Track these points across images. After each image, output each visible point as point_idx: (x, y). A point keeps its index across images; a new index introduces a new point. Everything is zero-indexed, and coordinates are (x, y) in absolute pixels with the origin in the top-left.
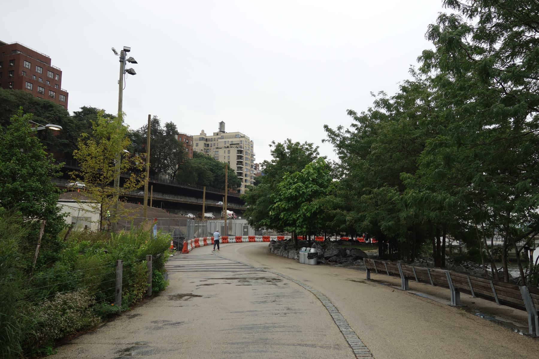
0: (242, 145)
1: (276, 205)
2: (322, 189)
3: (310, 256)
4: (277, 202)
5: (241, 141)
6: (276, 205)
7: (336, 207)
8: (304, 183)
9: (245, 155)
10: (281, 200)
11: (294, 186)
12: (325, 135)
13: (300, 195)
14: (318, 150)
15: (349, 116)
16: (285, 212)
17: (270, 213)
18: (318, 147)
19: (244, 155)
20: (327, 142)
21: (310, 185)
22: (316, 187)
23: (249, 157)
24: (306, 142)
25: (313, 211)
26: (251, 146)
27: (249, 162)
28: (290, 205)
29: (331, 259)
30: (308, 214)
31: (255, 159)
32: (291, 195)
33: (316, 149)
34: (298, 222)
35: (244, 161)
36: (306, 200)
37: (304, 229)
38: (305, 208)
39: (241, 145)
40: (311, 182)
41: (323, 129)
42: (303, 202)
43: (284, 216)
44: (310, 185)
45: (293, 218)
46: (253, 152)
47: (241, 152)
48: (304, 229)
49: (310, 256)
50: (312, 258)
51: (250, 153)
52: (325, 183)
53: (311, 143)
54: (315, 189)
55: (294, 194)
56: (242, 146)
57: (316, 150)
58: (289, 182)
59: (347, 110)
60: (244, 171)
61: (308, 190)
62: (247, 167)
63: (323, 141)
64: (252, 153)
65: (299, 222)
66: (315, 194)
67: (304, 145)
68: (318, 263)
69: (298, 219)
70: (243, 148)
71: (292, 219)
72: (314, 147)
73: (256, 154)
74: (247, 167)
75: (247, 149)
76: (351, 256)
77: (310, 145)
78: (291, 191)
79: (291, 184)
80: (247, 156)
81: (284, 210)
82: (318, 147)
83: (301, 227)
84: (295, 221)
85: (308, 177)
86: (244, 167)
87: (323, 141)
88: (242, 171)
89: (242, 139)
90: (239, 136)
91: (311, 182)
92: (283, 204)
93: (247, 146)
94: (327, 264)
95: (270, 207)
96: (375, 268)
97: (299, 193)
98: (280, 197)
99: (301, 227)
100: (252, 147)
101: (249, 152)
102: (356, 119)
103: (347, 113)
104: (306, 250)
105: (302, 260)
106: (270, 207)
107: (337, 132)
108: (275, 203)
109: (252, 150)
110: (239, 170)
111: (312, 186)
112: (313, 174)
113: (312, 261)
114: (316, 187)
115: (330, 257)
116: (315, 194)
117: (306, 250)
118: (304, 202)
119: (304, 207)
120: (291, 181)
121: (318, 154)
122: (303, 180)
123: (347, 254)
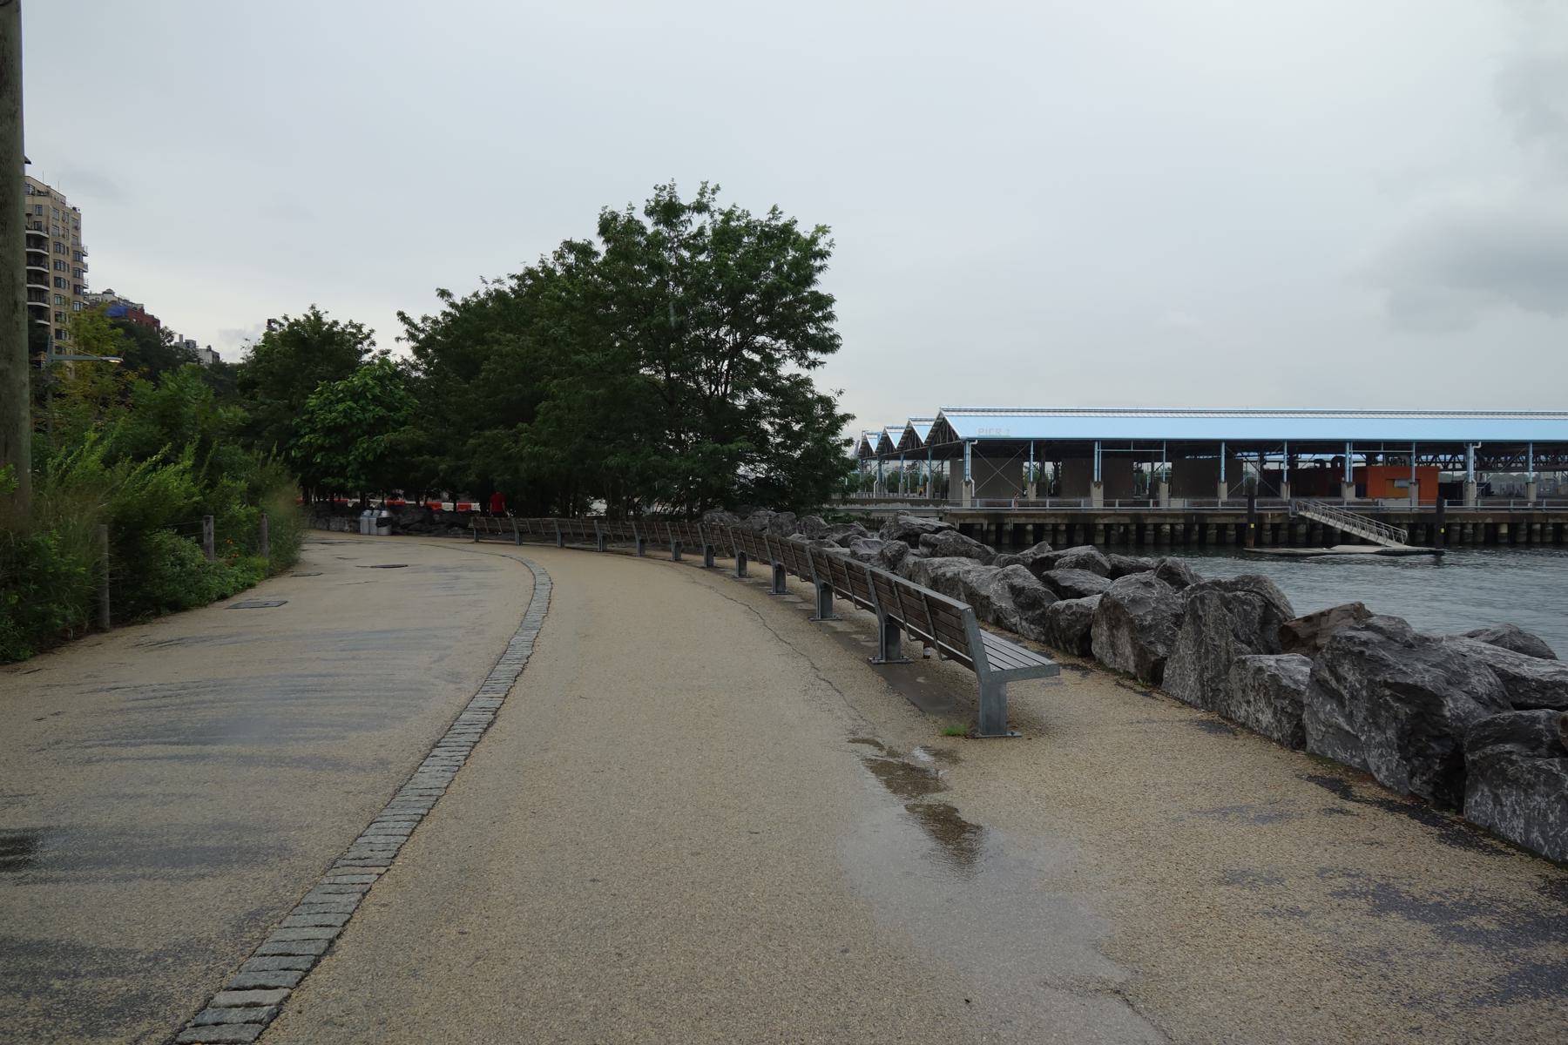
0: (43, 220)
1: (306, 439)
2: (392, 414)
3: (381, 522)
4: (306, 434)
5: (39, 207)
6: (306, 439)
7: (419, 449)
8: (356, 402)
9: (55, 252)
10: (313, 431)
11: (340, 407)
12: (401, 329)
13: (353, 424)
14: (373, 337)
15: (439, 298)
16: (323, 453)
17: (293, 454)
18: (372, 331)
19: (51, 255)
20: (404, 341)
21: (372, 408)
22: (381, 411)
23: (68, 259)
24: (351, 322)
25: (379, 452)
26: (71, 224)
27: (66, 276)
28: (333, 442)
29: (410, 527)
30: (370, 457)
31: (86, 266)
32: (336, 423)
33: (369, 335)
34: (350, 468)
35: (52, 274)
36: (365, 433)
37: (362, 483)
38: (365, 446)
39: (38, 219)
40: (369, 401)
41: (396, 317)
42: (359, 436)
43: (322, 459)
44: (372, 408)
45: (340, 463)
46: (79, 244)
47: (39, 241)
48: (362, 483)
49: (381, 522)
50: (385, 525)
51: (69, 245)
52: (396, 404)
53: (361, 323)
54: (381, 414)
55: (343, 421)
56: (44, 224)
57: (368, 336)
58: (327, 398)
59: (437, 290)
60: (52, 305)
61: (367, 415)
62: (62, 292)
63: (398, 339)
64: (76, 248)
65: (352, 470)
66: (379, 425)
67: (346, 326)
68: (393, 533)
69: (349, 463)
70: (47, 229)
71: (337, 464)
72: (365, 330)
73: (89, 252)
74: (62, 292)
75: (61, 232)
76: (443, 523)
77: (359, 328)
78: (335, 415)
79: (331, 402)
80: (61, 257)
81: (321, 448)
82: (372, 331)
83: (357, 478)
84: (343, 468)
85: (365, 393)
86: (51, 289)
87: (398, 339)
88: (44, 302)
89: (39, 200)
90: (31, 190)
91: (369, 401)
92: (317, 439)
93: (60, 224)
94: (408, 534)
95: (292, 442)
96: (486, 527)
97: (351, 420)
98: (310, 425)
99: (357, 478)
100: (77, 228)
101: (68, 244)
102: (453, 305)
103: (436, 293)
104: (372, 514)
105: (364, 527)
106: (292, 442)
107: (421, 325)
108: (303, 436)
109: (77, 238)
110: (33, 298)
111: (374, 409)
112: (373, 387)
113: (384, 530)
114: (381, 411)
115: (410, 525)
116: (379, 425)
117: (372, 514)
118: (361, 436)
119: (363, 445)
120: (332, 397)
121: (373, 343)
122: (356, 395)
123: (434, 520)
